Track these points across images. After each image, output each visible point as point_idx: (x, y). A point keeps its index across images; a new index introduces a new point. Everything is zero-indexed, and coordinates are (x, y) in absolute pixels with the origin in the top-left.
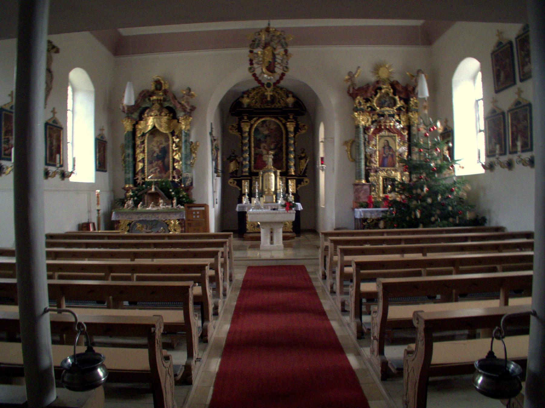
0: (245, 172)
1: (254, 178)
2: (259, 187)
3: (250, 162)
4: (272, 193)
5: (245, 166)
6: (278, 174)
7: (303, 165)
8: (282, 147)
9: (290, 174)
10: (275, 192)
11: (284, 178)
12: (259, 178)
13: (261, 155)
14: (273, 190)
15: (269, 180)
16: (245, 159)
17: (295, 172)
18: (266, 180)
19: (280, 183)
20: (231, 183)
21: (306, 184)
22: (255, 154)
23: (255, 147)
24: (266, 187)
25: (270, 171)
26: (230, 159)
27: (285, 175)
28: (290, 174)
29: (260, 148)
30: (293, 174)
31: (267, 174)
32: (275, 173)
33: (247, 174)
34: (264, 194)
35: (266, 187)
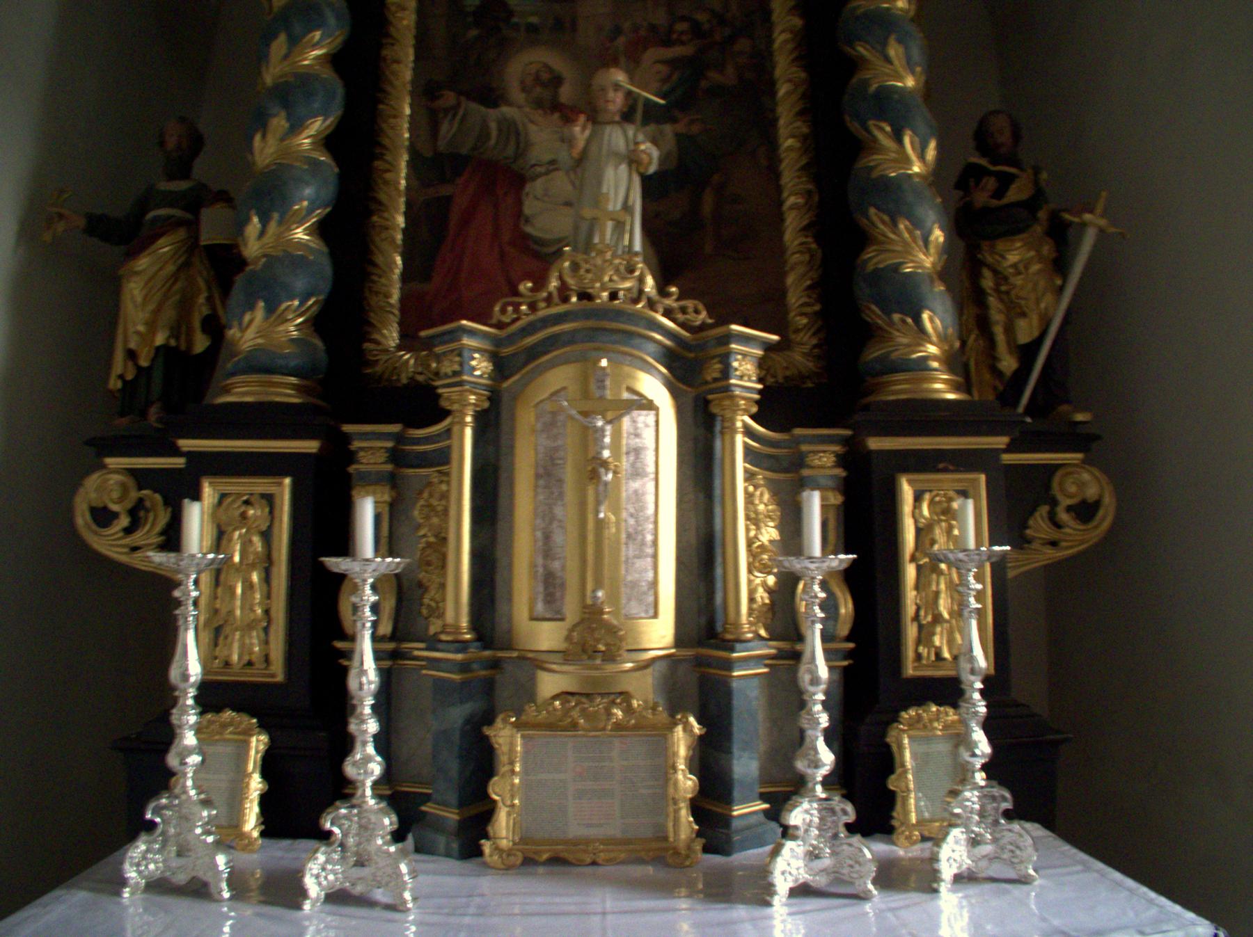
0: (262, 364)
1: (371, 445)
2: (408, 600)
3: (348, 229)
5: (269, 290)
6: (745, 372)
7: (1035, 298)
8: (758, 85)
9: (899, 389)
11: (824, 460)
12: (443, 458)
13: (506, 178)
14: (659, 632)
15: (593, 468)
16: (270, 194)
18: (547, 474)
19: (778, 541)
20: (102, 517)
21: (1078, 537)
22: (433, 166)
23: (426, 92)
24: (551, 586)
25: (606, 327)
26: (124, 233)
27: (834, 399)
28: (899, 389)
29: (491, 97)
30: (942, 388)
31: (558, 378)
32: (695, 377)
33: (285, 391)
34: (528, 692)
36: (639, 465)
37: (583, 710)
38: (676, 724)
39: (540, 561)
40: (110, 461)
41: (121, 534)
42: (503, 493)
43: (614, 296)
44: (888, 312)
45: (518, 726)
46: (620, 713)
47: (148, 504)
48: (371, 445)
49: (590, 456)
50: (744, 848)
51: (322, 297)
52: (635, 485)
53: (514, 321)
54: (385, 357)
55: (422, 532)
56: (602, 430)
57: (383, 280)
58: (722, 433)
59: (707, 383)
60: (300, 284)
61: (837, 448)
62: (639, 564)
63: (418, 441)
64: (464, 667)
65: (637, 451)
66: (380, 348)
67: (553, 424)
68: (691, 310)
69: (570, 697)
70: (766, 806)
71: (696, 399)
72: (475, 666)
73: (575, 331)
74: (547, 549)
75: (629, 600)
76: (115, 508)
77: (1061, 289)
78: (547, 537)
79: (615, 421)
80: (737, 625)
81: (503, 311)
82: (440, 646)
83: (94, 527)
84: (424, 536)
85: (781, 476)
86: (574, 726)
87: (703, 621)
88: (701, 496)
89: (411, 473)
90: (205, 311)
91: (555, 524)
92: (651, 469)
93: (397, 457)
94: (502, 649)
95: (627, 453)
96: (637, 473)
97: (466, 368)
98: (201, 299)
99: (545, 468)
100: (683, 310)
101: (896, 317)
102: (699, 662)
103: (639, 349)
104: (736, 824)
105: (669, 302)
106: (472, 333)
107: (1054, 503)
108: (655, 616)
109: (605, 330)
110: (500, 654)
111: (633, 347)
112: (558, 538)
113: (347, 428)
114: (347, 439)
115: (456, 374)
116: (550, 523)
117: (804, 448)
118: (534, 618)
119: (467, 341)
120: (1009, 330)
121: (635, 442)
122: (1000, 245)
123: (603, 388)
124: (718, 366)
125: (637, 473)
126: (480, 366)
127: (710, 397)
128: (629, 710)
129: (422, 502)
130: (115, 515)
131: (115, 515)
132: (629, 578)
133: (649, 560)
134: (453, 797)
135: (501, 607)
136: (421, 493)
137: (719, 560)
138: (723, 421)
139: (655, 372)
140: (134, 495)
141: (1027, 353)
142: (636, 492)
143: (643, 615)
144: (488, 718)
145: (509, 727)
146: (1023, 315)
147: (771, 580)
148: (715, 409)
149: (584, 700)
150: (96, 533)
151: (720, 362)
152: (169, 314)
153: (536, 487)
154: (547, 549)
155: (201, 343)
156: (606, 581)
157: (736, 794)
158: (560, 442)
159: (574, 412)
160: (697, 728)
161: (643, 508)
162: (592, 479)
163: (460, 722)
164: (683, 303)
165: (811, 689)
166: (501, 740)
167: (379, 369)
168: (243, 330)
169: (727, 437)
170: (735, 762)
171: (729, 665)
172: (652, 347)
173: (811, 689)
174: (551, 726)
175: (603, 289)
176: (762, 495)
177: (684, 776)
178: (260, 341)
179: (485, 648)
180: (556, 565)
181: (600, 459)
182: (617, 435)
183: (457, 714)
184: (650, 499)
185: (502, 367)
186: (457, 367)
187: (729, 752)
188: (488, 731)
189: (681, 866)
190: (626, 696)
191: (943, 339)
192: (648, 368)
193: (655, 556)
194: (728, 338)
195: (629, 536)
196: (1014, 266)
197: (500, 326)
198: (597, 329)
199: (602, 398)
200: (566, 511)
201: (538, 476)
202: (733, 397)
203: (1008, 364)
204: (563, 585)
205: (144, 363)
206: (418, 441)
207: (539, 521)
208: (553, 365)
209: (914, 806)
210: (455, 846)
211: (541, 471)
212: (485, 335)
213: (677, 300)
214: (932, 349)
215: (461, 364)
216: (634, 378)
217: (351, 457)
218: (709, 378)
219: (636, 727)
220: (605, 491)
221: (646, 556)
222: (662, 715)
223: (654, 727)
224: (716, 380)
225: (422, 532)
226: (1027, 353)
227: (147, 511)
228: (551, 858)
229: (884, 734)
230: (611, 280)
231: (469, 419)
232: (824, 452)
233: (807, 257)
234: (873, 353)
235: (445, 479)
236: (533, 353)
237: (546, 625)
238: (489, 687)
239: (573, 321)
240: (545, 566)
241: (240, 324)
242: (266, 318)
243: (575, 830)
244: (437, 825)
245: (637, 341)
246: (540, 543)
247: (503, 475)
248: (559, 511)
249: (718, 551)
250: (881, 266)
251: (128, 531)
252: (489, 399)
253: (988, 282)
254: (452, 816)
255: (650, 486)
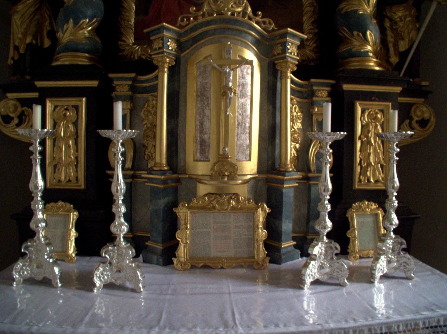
0: (73, 48)
1: (122, 82)
4: (244, 192)
6: (292, 51)
9: (354, 64)
10: (268, 185)
11: (322, 93)
12: (154, 89)
14: (250, 167)
17: (382, 54)
18: (202, 95)
24: (203, 146)
25: (229, 28)
27: (327, 68)
30: (373, 64)
31: (207, 51)
33: (83, 60)
34: (193, 193)
35: (203, 146)
36: (243, 91)
37: (218, 201)
38: (258, 208)
39: (198, 135)
40: (9, 95)
41: (15, 127)
42: (181, 103)
43: (233, 14)
44: (351, 31)
45: (189, 208)
46: (234, 203)
47: (26, 113)
48: (122, 82)
49: (222, 86)
50: (286, 261)
51: (99, 19)
52: (242, 100)
53: (187, 25)
54: (127, 48)
55: (144, 123)
56: (229, 73)
57: (127, 14)
58: (281, 79)
59: (275, 55)
60: (90, 12)
61: (328, 89)
62: (243, 136)
63: (143, 82)
64: (164, 182)
65: (243, 85)
66: (126, 43)
67: (205, 71)
68: (268, 23)
69: (212, 195)
70: (295, 243)
71: (269, 64)
72: (169, 181)
73: (215, 30)
74: (201, 130)
75: (238, 153)
76: (12, 115)
77: (419, 30)
78: (202, 124)
79: (234, 70)
80: (286, 165)
81: (182, 20)
82: (153, 172)
83: (3, 124)
84: (146, 124)
85: (304, 100)
86: (214, 208)
87: (270, 163)
88: (271, 108)
89: (140, 97)
90: (49, 28)
91: (205, 118)
92: (249, 94)
93: (133, 88)
94: (181, 174)
95: (239, 86)
96: (243, 95)
97: (165, 46)
98: (47, 23)
99: (201, 92)
100: (264, 23)
101: (355, 33)
102: (268, 181)
103: (245, 38)
104: (283, 251)
105: (258, 19)
106: (168, 29)
107: (411, 119)
108: (250, 160)
109: (230, 29)
110: (180, 176)
111: (241, 37)
112: (207, 124)
113: (111, 75)
114: (111, 80)
115: (160, 48)
116: (203, 118)
117: (315, 88)
118: (195, 160)
119: (166, 33)
120: (396, 45)
121: (242, 81)
122: (394, 9)
123: (230, 54)
124: (281, 48)
125: (243, 95)
126: (171, 45)
127: (276, 62)
128: (238, 201)
129: (144, 109)
130: (12, 119)
131: (12, 119)
132: (238, 143)
133: (247, 135)
134: (160, 239)
135: (181, 156)
136: (144, 105)
137: (278, 136)
138: (281, 73)
139: (251, 49)
140: (20, 109)
141: (403, 56)
142: (242, 104)
143: (244, 159)
144: (175, 204)
145: (185, 208)
146: (403, 39)
147: (298, 146)
148: (278, 68)
149: (218, 197)
150: (4, 126)
151: (281, 46)
152: (33, 29)
153: (197, 101)
154: (201, 130)
155: (47, 43)
156: (229, 144)
157: (283, 238)
158: (207, 80)
159: (215, 65)
160: (268, 210)
161: (245, 111)
162: (224, 96)
163: (163, 206)
164: (264, 19)
165: (324, 194)
166: (181, 214)
167: (125, 53)
168: (64, 33)
169: (283, 81)
170: (283, 224)
171: (282, 182)
172: (250, 38)
173: (324, 194)
174: (203, 208)
175: (229, 10)
176: (295, 108)
177: (262, 230)
178: (71, 37)
179: (174, 173)
180: (206, 137)
181: (228, 87)
182: (235, 76)
183: (162, 202)
184: (249, 107)
185: (181, 46)
186: (161, 45)
187: (281, 220)
188: (175, 210)
189: (260, 269)
190: (237, 195)
191: (374, 44)
192: (248, 47)
193: (250, 134)
194: (285, 35)
195: (239, 124)
196: (400, 17)
197: (181, 27)
198: (224, 29)
199: (229, 59)
200: (211, 112)
201: (197, 96)
202: (287, 62)
203: (394, 60)
204: (209, 146)
205: (22, 52)
206: (143, 82)
207: (198, 116)
208: (205, 45)
209: (356, 245)
210: (161, 260)
211: (199, 94)
212: (174, 31)
213: (261, 18)
214: (369, 48)
215: (163, 44)
216: (242, 51)
217: (113, 89)
218: (276, 53)
219: (241, 209)
220: (230, 102)
221: (246, 133)
222: (252, 204)
223: (248, 208)
224: (279, 54)
225: (144, 123)
226: (403, 56)
227: (26, 116)
228: (204, 265)
229: (345, 213)
230: (232, 6)
231: (166, 70)
232: (323, 90)
233: (312, 9)
234: (344, 49)
235: (155, 98)
236: (195, 40)
237: (201, 164)
238: (176, 190)
239: (215, 24)
240: (200, 137)
241: (62, 31)
242: (74, 27)
243: (214, 253)
244: (153, 251)
245: (244, 35)
246: (198, 127)
247: (181, 97)
248: (207, 112)
249: (278, 132)
250: (349, 10)
251: (18, 125)
252: (175, 61)
253: (387, 24)
254: (159, 247)
255: (249, 101)
